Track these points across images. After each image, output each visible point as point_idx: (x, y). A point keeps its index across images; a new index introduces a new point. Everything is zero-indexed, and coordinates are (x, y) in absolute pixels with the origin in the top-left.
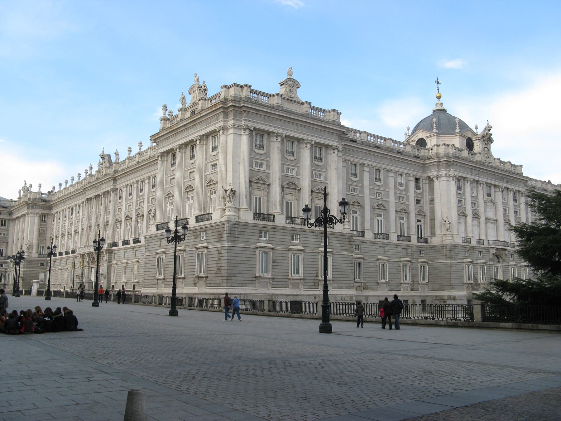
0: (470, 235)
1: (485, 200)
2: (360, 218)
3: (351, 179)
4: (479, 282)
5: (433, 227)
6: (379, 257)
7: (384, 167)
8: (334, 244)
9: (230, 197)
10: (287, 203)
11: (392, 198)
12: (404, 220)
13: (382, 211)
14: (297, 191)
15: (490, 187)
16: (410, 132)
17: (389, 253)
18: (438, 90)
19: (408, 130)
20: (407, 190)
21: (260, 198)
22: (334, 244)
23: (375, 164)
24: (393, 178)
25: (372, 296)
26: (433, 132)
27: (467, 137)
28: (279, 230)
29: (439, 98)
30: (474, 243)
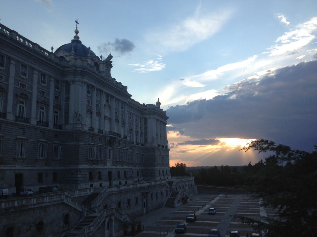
0: (93, 126)
1: (105, 104)
4: (98, 159)
5: (67, 118)
6: (18, 137)
12: (43, 110)
15: (108, 96)
16: (54, 52)
18: (77, 27)
19: (52, 48)
23: (21, 60)
25: (8, 170)
26: (72, 53)
27: (95, 61)
29: (77, 32)
30: (96, 131)
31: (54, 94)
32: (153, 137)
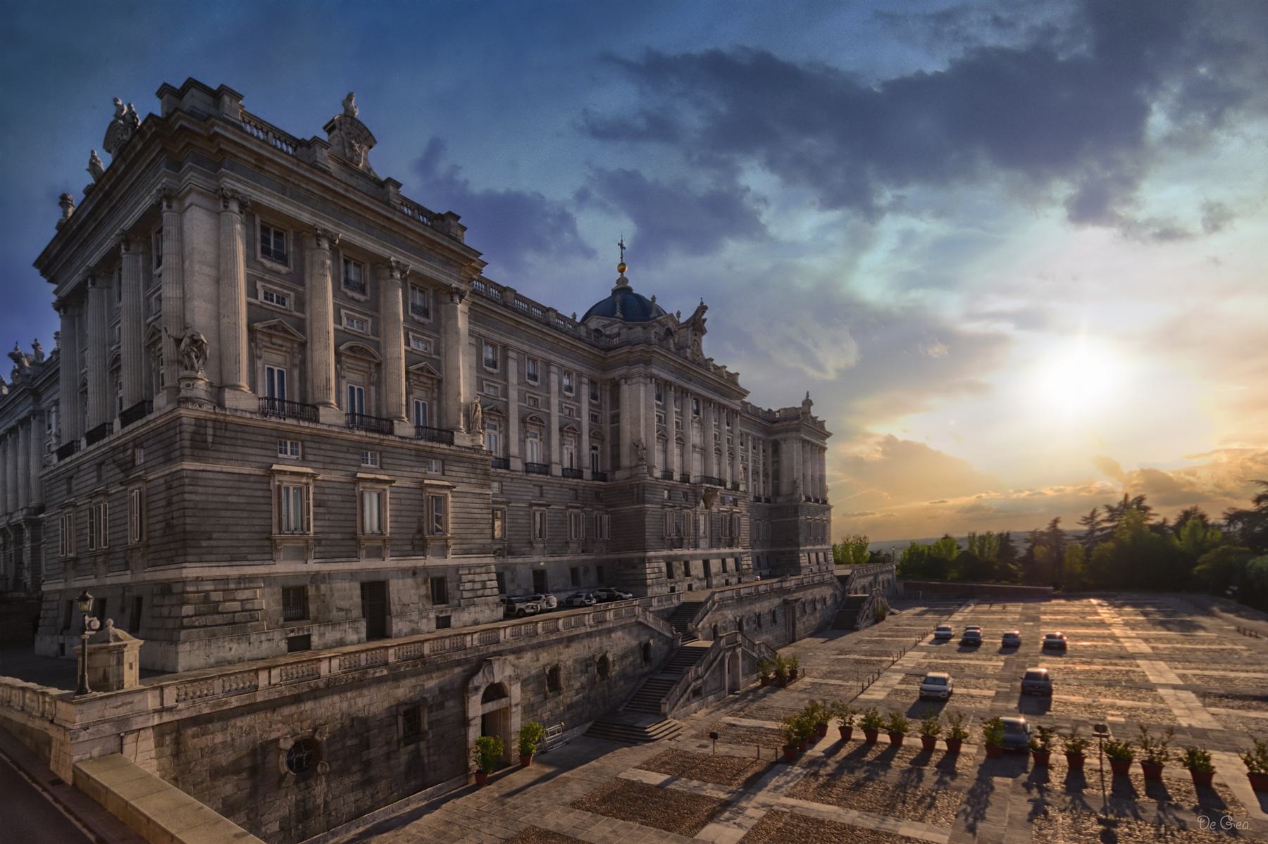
0: (670, 467)
2: (501, 435)
3: (485, 370)
5: (616, 457)
7: (542, 356)
8: (454, 474)
9: (189, 357)
10: (352, 389)
11: (555, 410)
13: (538, 428)
14: (372, 366)
17: (549, 496)
20: (578, 399)
21: (281, 373)
22: (454, 474)
24: (556, 376)
28: (330, 441)
30: (677, 476)
31: (590, 410)
32: (795, 482)
